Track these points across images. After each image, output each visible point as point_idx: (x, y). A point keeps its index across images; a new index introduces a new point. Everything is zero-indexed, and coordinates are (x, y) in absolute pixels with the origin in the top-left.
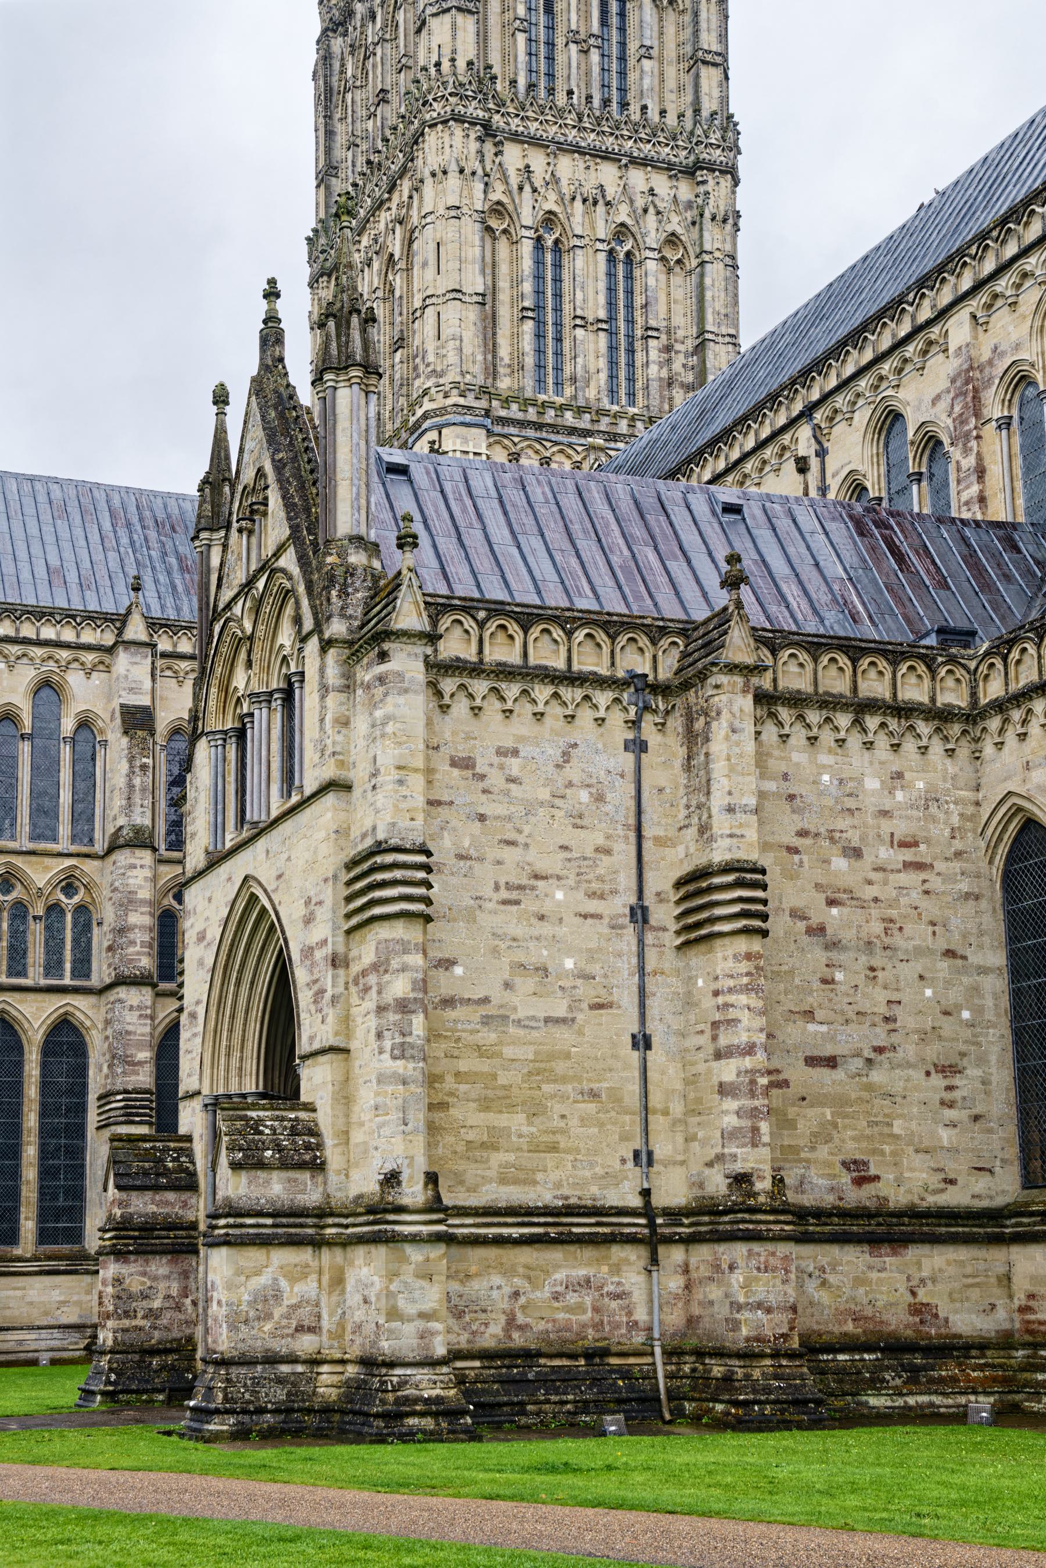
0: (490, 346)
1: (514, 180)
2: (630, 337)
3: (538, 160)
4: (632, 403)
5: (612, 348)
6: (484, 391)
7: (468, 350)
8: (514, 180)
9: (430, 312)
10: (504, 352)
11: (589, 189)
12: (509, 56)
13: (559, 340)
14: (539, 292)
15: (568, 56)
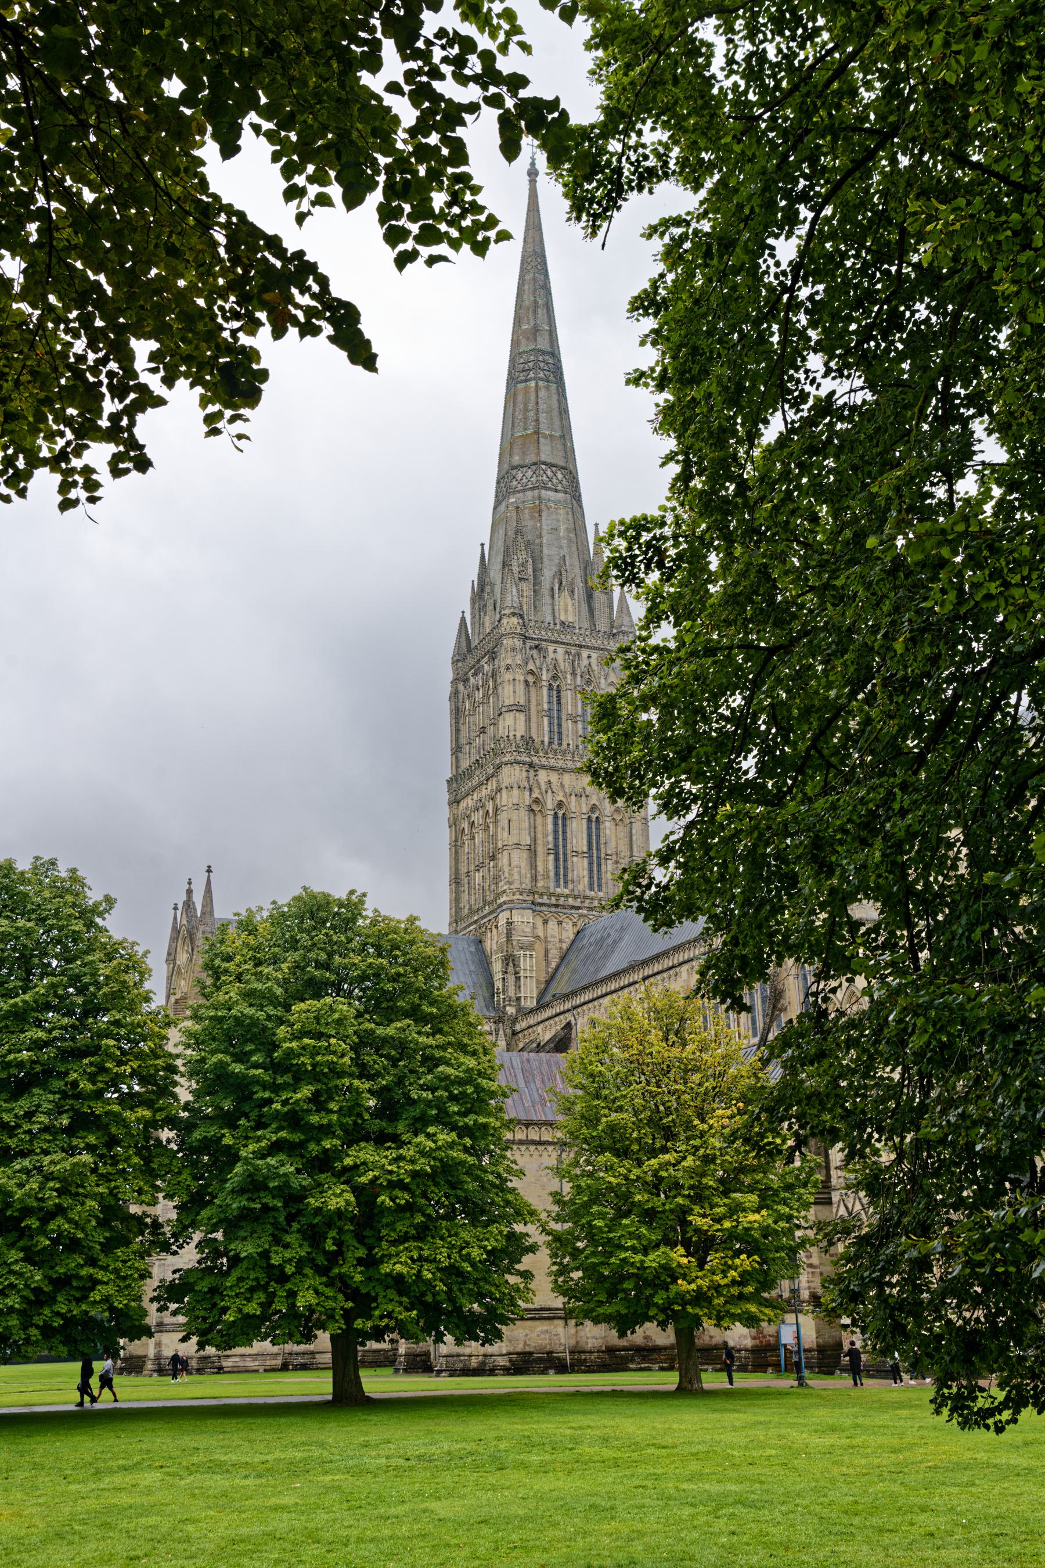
0: (533, 866)
1: (543, 787)
2: (599, 858)
3: (554, 777)
4: (600, 890)
5: (591, 864)
6: (531, 892)
7: (523, 872)
8: (543, 787)
9: (506, 853)
10: (540, 869)
11: (578, 789)
12: (540, 727)
13: (565, 861)
14: (556, 839)
15: (568, 725)
